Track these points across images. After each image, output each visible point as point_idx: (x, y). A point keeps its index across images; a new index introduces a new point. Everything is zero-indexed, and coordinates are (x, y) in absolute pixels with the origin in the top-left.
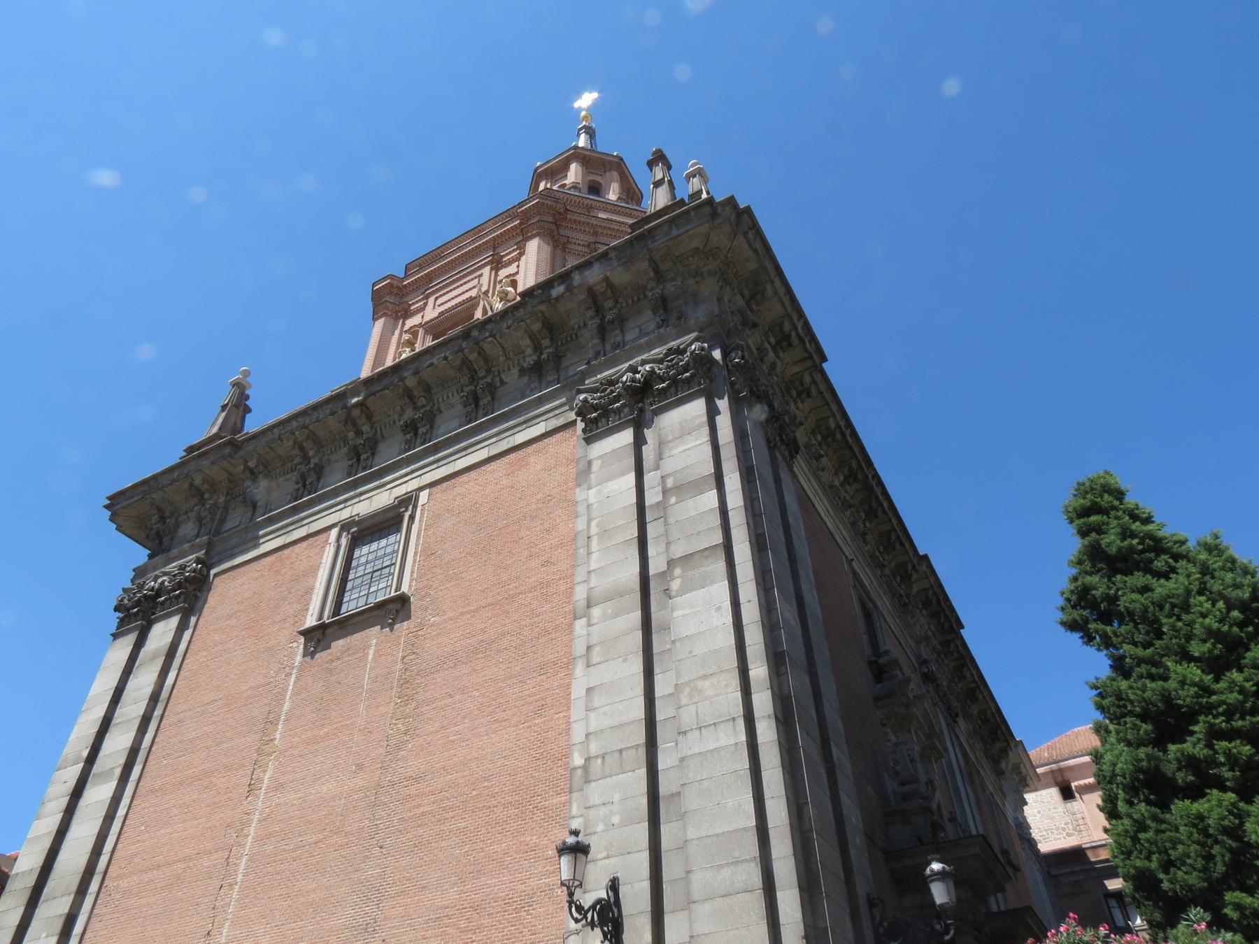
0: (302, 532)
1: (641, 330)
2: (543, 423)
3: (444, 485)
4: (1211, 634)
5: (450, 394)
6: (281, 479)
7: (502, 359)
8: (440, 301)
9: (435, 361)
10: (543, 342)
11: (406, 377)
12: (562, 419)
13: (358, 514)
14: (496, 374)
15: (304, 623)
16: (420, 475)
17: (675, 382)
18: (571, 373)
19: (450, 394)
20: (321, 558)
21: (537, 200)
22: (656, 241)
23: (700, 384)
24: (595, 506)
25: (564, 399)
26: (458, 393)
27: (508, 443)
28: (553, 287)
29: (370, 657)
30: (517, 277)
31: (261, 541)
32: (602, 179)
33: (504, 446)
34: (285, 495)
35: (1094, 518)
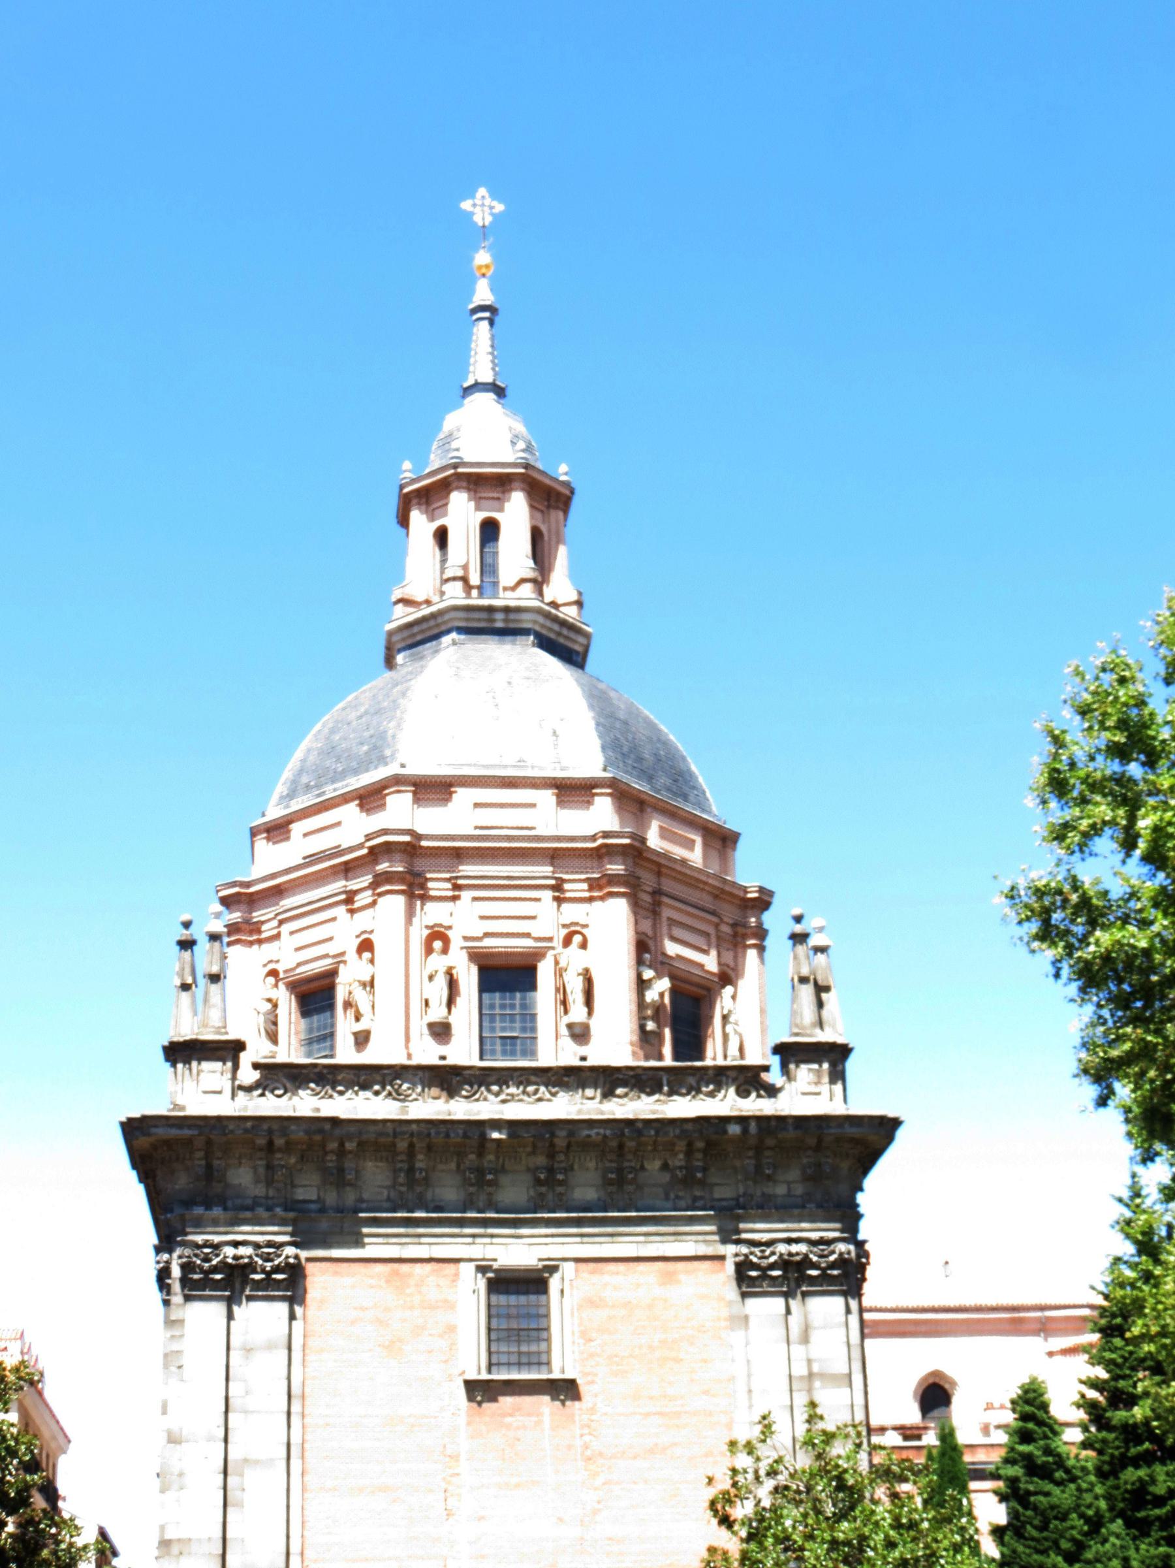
1: (789, 1190)
2: (692, 1244)
3: (592, 1265)
4: (1073, 1540)
6: (370, 1164)
7: (650, 1148)
9: (593, 1132)
11: (558, 1137)
13: (495, 1260)
16: (563, 1244)
17: (824, 1278)
18: (717, 1195)
19: (588, 1158)
21: (627, 841)
23: (841, 1285)
25: (713, 1228)
27: (658, 1249)
31: (367, 1240)
32: (544, 522)
34: (380, 1186)
35: (1031, 1425)
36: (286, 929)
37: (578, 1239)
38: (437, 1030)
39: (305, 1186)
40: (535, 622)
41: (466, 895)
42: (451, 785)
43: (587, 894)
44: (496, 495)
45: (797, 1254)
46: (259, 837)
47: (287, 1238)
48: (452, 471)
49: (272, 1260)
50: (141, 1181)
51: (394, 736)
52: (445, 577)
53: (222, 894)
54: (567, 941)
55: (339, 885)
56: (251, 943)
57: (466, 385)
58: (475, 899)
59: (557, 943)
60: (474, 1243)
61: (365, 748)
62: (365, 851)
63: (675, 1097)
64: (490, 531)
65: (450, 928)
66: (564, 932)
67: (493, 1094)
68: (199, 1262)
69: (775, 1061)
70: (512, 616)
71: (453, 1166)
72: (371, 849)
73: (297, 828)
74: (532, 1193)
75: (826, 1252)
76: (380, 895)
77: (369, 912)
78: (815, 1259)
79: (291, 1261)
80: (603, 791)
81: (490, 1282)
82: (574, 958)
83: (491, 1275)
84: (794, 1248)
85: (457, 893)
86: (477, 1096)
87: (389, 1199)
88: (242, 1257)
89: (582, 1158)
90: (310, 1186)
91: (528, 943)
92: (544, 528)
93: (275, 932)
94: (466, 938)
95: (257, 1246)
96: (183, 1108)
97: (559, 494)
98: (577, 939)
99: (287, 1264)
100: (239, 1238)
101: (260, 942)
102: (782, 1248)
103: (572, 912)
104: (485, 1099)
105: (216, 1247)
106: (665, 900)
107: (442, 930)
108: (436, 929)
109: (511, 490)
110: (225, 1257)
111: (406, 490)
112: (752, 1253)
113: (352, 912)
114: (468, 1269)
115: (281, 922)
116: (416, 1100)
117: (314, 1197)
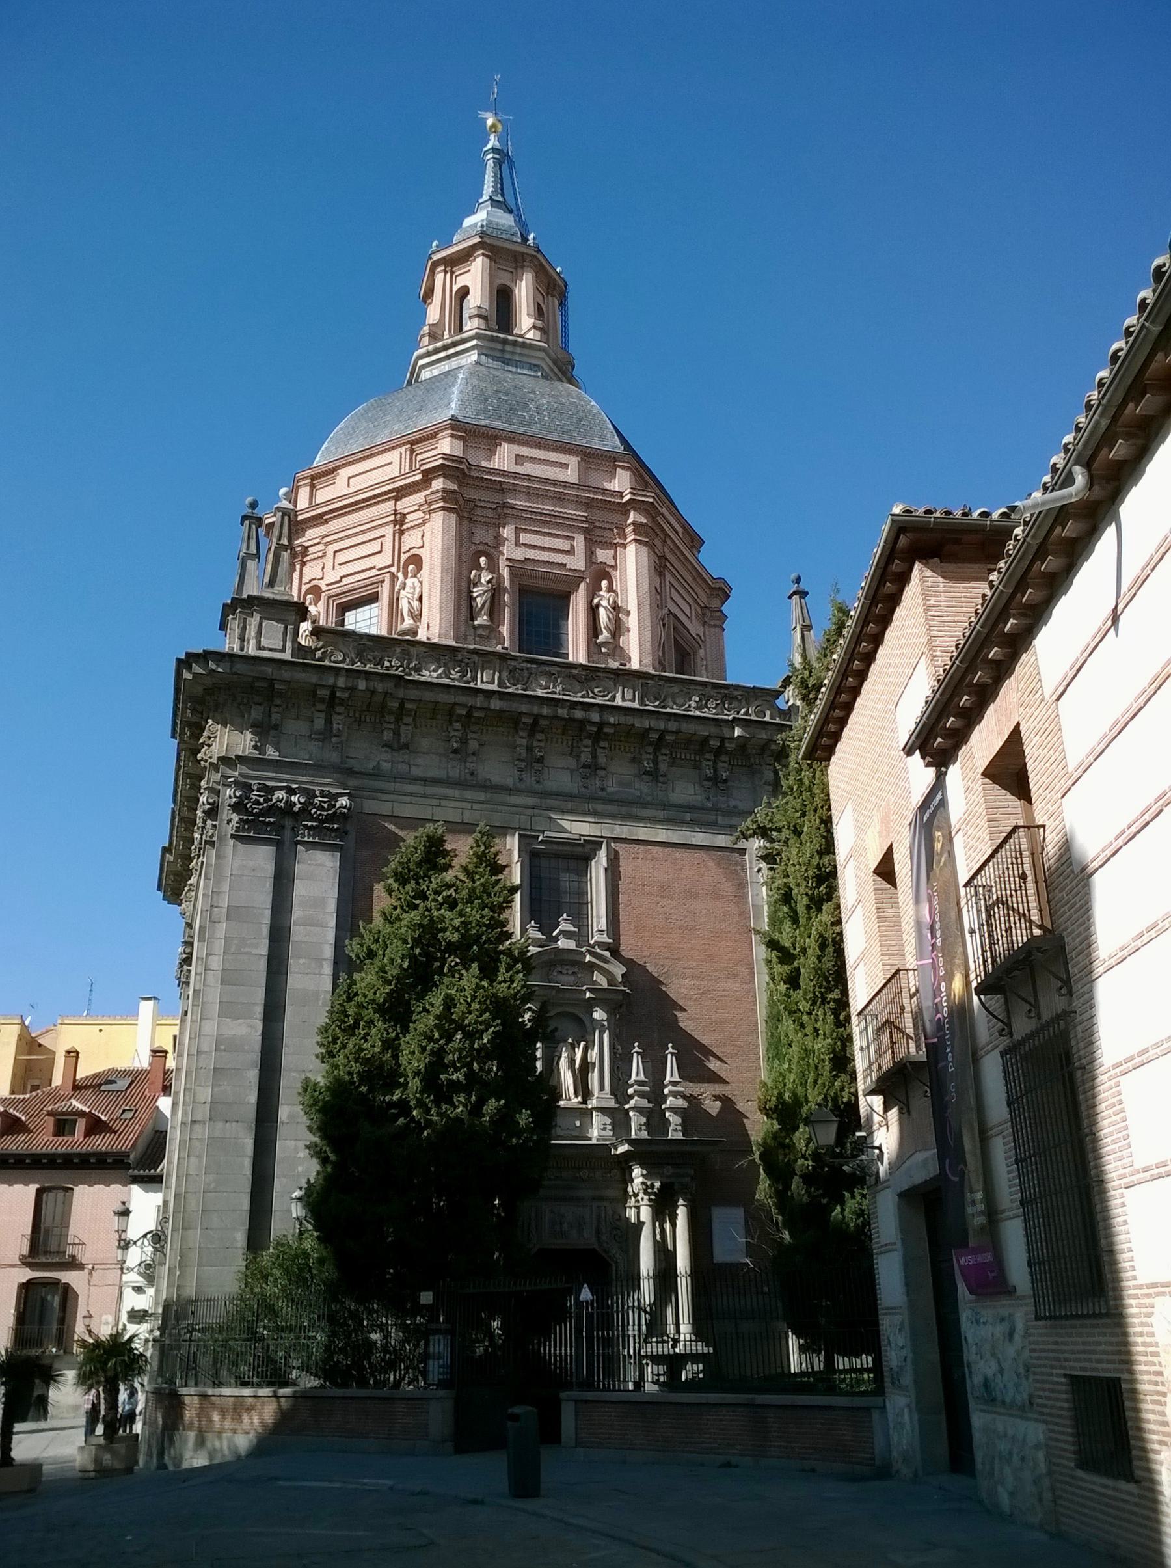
8: (525, 538)
21: (651, 500)
30: (613, 573)
38: (480, 632)
40: (543, 359)
42: (496, 437)
48: (477, 240)
55: (388, 506)
57: (481, 201)
62: (419, 477)
64: (503, 298)
70: (526, 351)
72: (426, 473)
73: (344, 473)
76: (430, 512)
77: (418, 533)
92: (544, 307)
93: (320, 554)
97: (555, 284)
103: (603, 555)
106: (668, 564)
109: (523, 267)
111: (436, 257)
113: (402, 532)
115: (326, 544)
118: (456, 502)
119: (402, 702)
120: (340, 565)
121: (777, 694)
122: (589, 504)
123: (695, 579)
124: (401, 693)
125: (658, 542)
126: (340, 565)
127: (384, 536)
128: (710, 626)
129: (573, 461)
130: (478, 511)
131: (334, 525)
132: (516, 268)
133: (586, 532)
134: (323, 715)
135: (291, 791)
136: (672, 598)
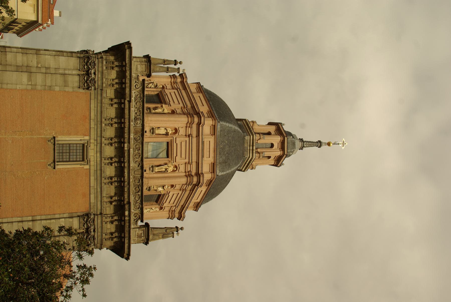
0: (92, 126)
5: (118, 172)
8: (183, 144)
10: (119, 202)
12: (92, 207)
13: (90, 146)
14: (118, 187)
15: (59, 135)
18: (107, 208)
20: (81, 135)
22: (127, 240)
24: (59, 221)
26: (118, 175)
27: (92, 192)
28: (128, 212)
29: (41, 161)
30: (177, 171)
33: (92, 191)
34: (110, 114)
36: (176, 91)
37: (96, 169)
39: (111, 93)
40: (249, 157)
41: (187, 139)
43: (187, 171)
44: (279, 147)
45: (91, 232)
46: (197, 84)
47: (96, 87)
49: (90, 83)
50: (108, 48)
51: (225, 120)
52: (260, 134)
53: (183, 74)
54: (176, 167)
56: (171, 82)
58: (186, 141)
59: (175, 163)
60: (95, 140)
61: (221, 113)
63: (134, 197)
65: (178, 134)
66: (178, 166)
67: (136, 146)
68: (90, 62)
69: (144, 224)
70: (251, 151)
71: (117, 135)
72: (199, 113)
73: (201, 95)
74: (109, 156)
75: (91, 240)
78: (89, 237)
79: (90, 88)
80: (213, 175)
81: (83, 145)
82: (171, 169)
83: (86, 145)
84: (92, 231)
85: (187, 136)
86: (135, 141)
87: (107, 116)
88: (91, 74)
89: (118, 171)
90: (111, 94)
91: (175, 155)
94: (176, 138)
95: (94, 79)
96: (133, 60)
98: (175, 169)
99: (89, 87)
100: (97, 73)
101: (171, 84)
102: (92, 227)
103: (182, 168)
104: (134, 144)
105: (94, 67)
106: (184, 192)
107: (178, 132)
108: (178, 131)
110: (91, 69)
112: (91, 219)
114: (87, 138)
115: (177, 89)
116: (134, 125)
117: (108, 95)
118: (191, 122)
119: (124, 103)
120: (170, 93)
121: (142, 221)
122: (198, 164)
123: (182, 206)
124: (127, 102)
125: (190, 187)
126: (170, 93)
127: (180, 104)
128: (169, 213)
129: (211, 160)
130: (190, 129)
131: (183, 92)
132: (279, 149)
133: (189, 162)
134: (118, 82)
135: (95, 74)
136: (174, 194)
